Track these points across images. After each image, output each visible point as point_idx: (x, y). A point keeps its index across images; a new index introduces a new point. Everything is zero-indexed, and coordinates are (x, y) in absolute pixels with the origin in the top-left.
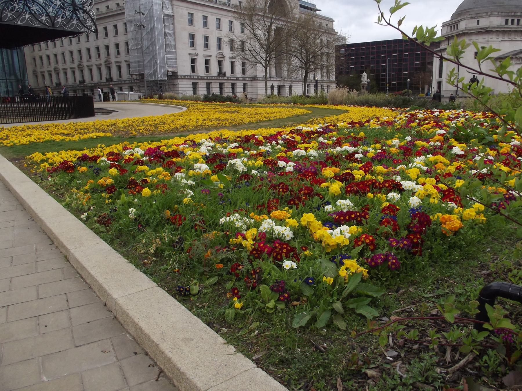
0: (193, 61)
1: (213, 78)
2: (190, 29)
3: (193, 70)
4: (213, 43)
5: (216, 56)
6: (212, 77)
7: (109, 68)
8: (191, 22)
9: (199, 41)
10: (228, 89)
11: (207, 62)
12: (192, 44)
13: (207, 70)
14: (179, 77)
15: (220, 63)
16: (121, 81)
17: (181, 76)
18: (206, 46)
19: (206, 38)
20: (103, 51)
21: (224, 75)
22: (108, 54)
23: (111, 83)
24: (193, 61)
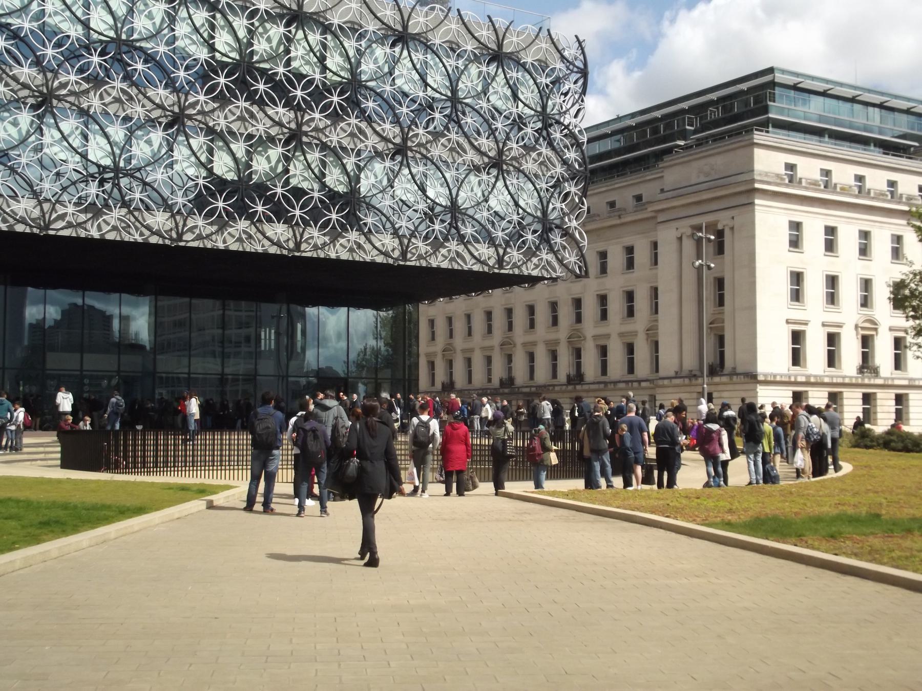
0: (797, 337)
1: (847, 381)
2: (795, 261)
3: (797, 358)
4: (849, 292)
5: (856, 327)
6: (844, 377)
7: (578, 353)
8: (795, 243)
9: (815, 288)
10: (886, 409)
11: (832, 339)
12: (797, 296)
13: (832, 360)
14: (761, 378)
15: (866, 342)
16: (605, 383)
17: (765, 375)
18: (832, 299)
19: (832, 281)
20: (566, 314)
21: (875, 371)
22: (579, 319)
23: (578, 387)
24: (797, 337)
